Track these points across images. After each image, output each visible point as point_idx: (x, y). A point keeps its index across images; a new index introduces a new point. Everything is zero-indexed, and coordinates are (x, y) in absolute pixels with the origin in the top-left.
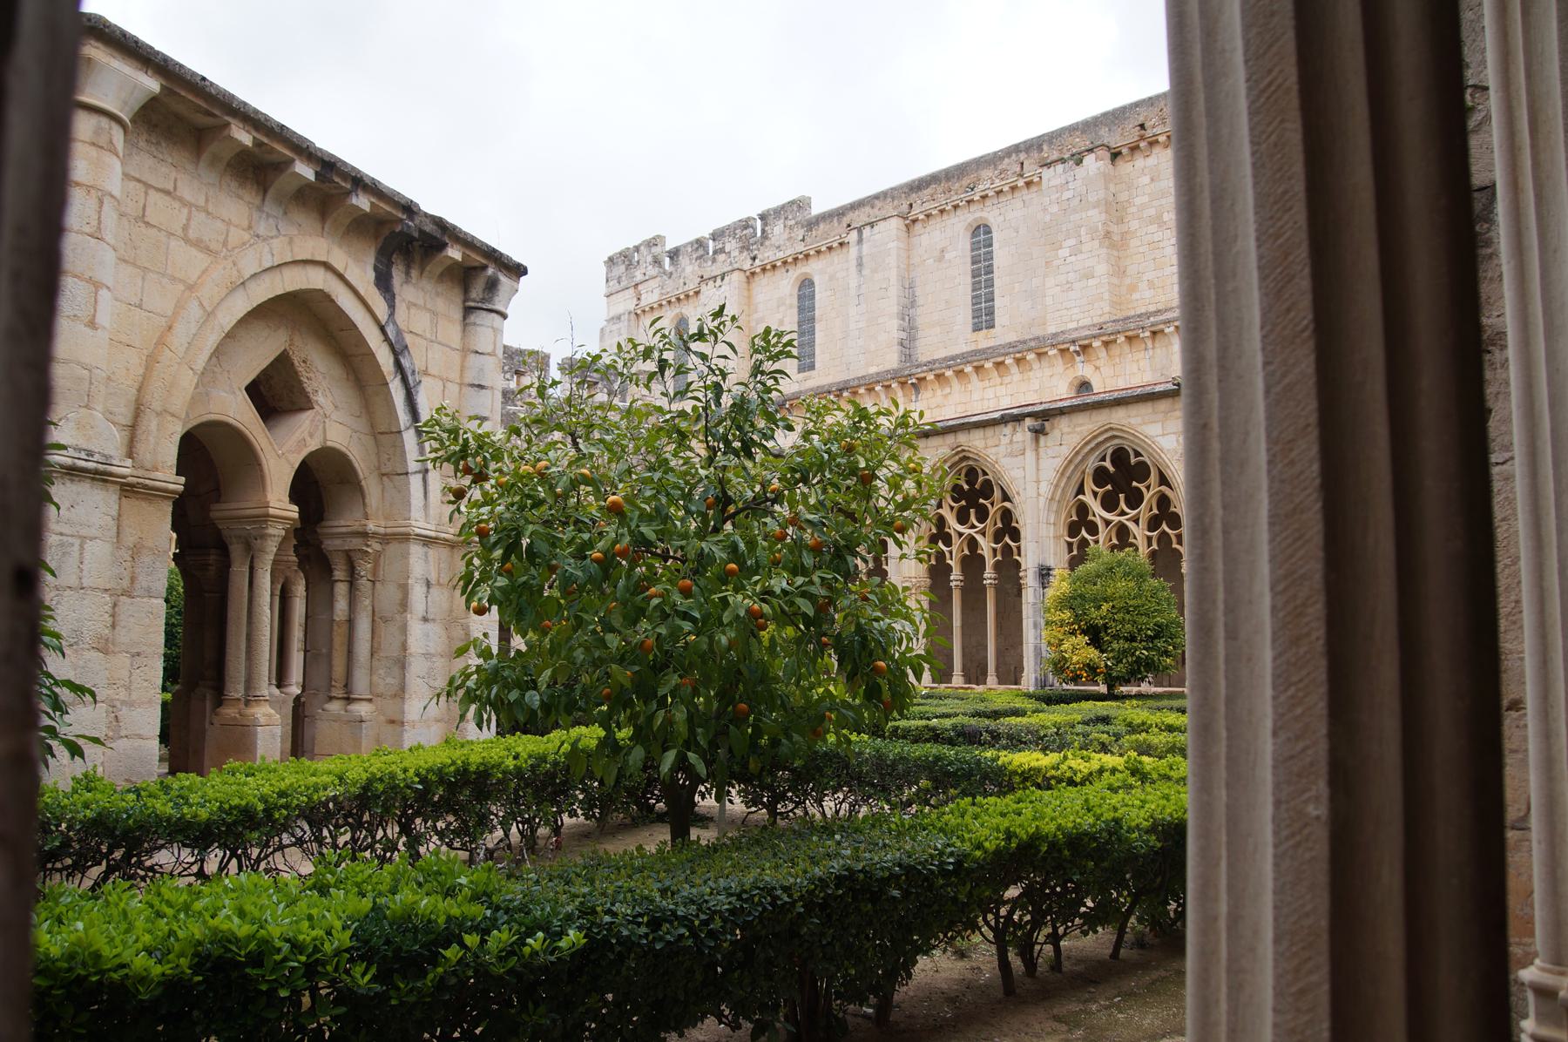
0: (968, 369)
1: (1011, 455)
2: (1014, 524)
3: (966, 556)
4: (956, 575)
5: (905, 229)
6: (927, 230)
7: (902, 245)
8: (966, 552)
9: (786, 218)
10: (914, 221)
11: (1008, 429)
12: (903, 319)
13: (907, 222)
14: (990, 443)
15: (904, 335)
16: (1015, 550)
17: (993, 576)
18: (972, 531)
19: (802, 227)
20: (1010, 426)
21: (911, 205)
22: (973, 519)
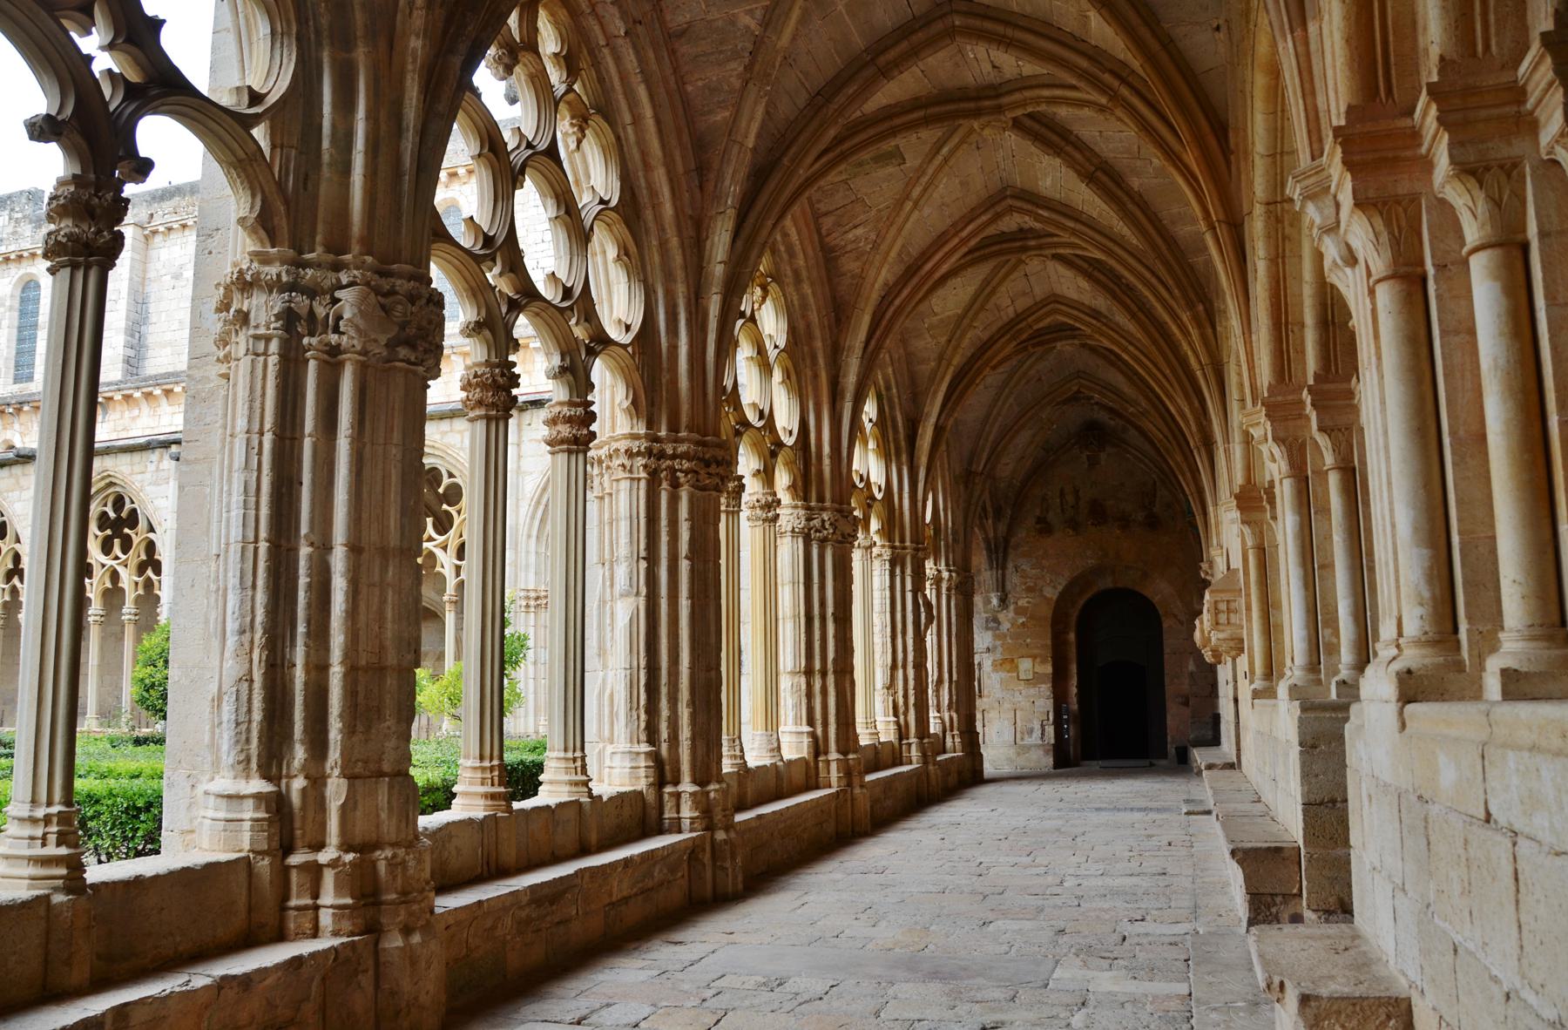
0: (157, 392)
1: (155, 483)
2: (156, 557)
3: (108, 589)
4: (95, 610)
5: (143, 239)
6: (168, 244)
7: (137, 257)
8: (109, 585)
9: (12, 210)
10: (155, 232)
11: (155, 456)
12: (132, 336)
13: (146, 232)
14: (137, 468)
15: (131, 353)
16: (156, 584)
17: (133, 611)
18: (114, 563)
19: (30, 222)
20: (158, 451)
21: (152, 215)
22: (117, 550)
